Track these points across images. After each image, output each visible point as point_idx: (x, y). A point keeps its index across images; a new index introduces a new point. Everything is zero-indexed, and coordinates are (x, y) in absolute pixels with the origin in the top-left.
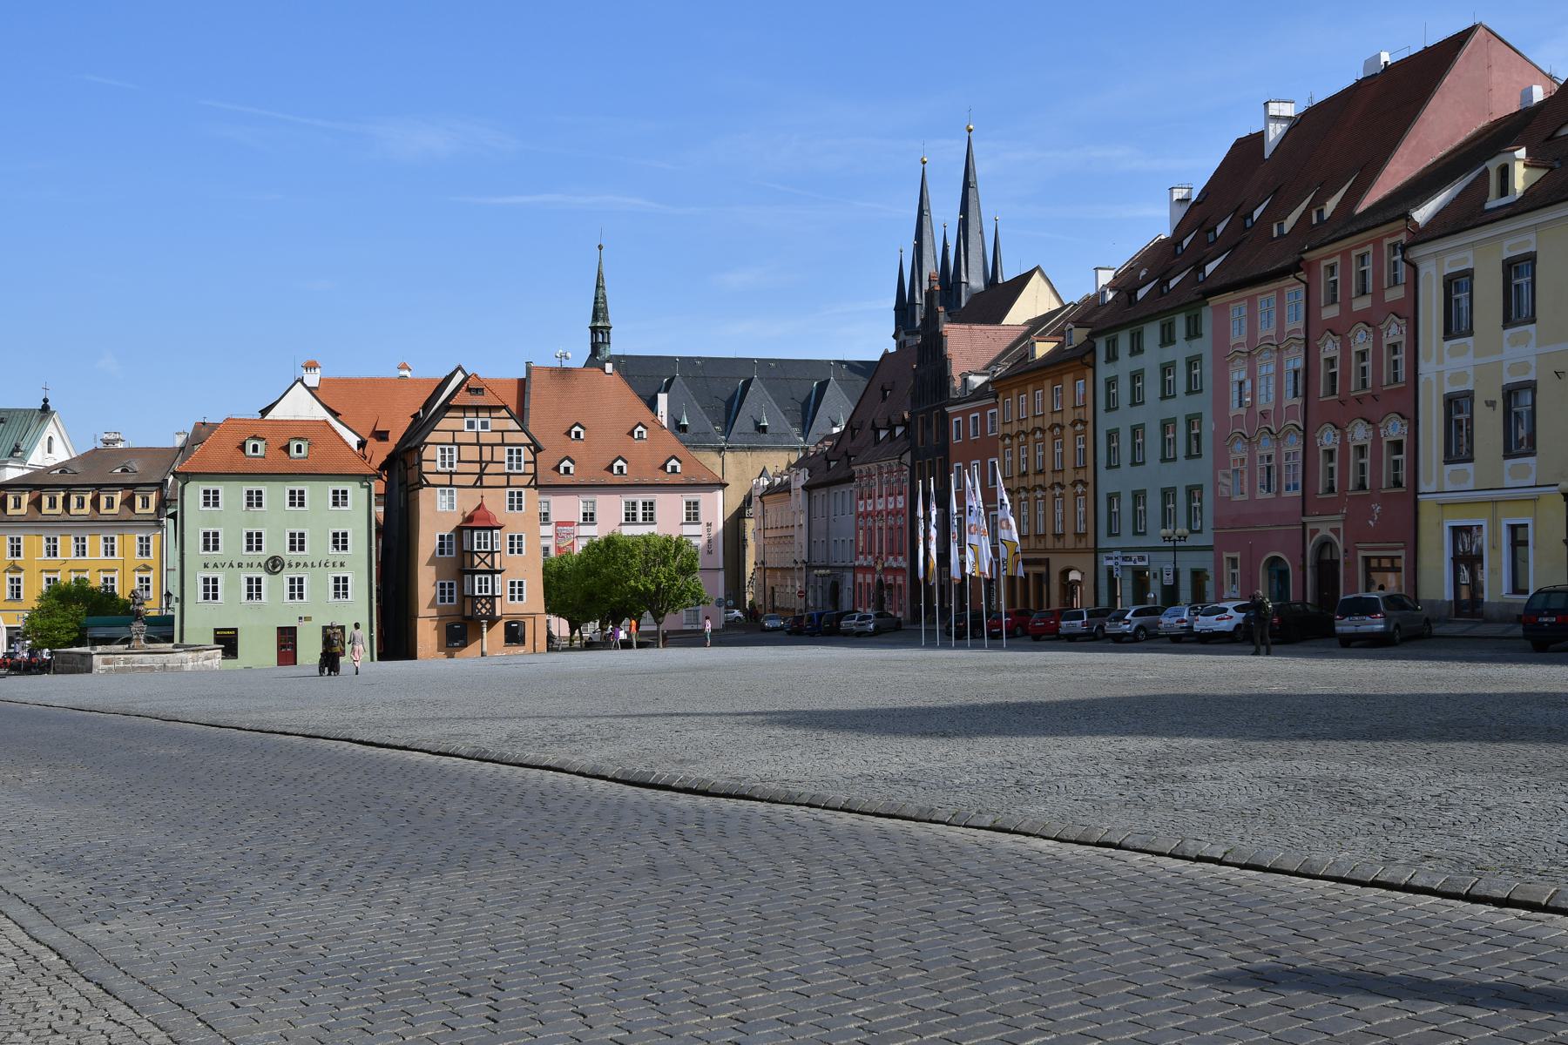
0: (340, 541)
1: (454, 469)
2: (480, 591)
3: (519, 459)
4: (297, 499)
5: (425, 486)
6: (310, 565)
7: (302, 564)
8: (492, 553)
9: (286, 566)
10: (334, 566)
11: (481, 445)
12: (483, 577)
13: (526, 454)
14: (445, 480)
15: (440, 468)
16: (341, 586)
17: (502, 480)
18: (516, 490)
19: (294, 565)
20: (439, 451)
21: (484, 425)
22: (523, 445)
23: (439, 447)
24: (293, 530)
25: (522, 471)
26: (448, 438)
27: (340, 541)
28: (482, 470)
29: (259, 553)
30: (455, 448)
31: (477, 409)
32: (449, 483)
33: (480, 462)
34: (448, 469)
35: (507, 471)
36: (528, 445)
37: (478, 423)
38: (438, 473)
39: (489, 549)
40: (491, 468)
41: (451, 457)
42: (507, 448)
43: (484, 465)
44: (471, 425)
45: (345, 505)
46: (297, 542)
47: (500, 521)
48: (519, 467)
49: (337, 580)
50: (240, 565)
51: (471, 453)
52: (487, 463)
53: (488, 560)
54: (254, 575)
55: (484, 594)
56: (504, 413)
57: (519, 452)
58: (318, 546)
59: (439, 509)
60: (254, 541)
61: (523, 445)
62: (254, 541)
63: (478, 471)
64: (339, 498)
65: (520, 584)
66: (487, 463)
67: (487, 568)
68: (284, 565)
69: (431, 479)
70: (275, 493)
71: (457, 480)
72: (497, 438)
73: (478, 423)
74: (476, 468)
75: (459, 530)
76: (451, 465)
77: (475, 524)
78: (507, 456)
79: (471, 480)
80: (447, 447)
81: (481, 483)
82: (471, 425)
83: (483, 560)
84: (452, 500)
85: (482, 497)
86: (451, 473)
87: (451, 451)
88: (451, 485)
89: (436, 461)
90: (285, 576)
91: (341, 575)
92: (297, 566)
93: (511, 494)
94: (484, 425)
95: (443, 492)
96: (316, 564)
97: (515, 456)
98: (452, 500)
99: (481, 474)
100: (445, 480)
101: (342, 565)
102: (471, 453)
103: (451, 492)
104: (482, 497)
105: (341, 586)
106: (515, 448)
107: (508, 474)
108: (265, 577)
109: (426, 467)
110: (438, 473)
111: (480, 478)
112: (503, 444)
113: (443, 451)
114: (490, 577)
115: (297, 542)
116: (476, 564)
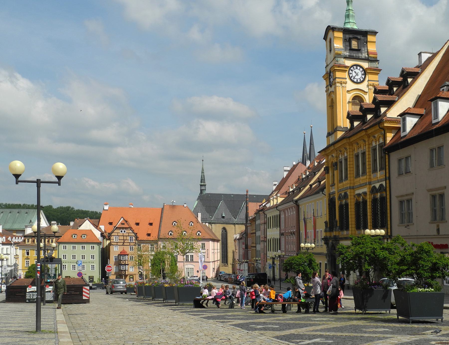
0: (93, 257)
1: (118, 241)
2: (123, 269)
3: (132, 239)
4: (83, 248)
11: (124, 236)
13: (134, 238)
14: (116, 244)
15: (115, 241)
16: (93, 267)
17: (129, 244)
18: (131, 246)
20: (114, 238)
21: (125, 232)
22: (133, 236)
23: (114, 236)
24: (82, 255)
25: (133, 242)
26: (116, 234)
27: (93, 257)
28: (124, 241)
29: (75, 259)
30: (118, 237)
31: (123, 228)
33: (124, 240)
34: (116, 241)
35: (129, 242)
36: (134, 236)
37: (123, 231)
40: (126, 241)
41: (117, 239)
42: (129, 237)
44: (122, 231)
45: (94, 249)
46: (83, 257)
47: (128, 253)
48: (132, 241)
49: (92, 266)
50: (71, 262)
51: (122, 238)
52: (125, 240)
56: (129, 229)
57: (132, 238)
58: (88, 258)
59: (115, 250)
60: (74, 257)
61: (133, 236)
62: (74, 257)
64: (93, 248)
66: (125, 240)
70: (79, 247)
71: (118, 244)
72: (127, 234)
73: (123, 231)
74: (123, 241)
75: (119, 255)
76: (117, 240)
77: (123, 254)
78: (129, 238)
79: (122, 244)
80: (116, 236)
82: (122, 231)
84: (117, 248)
86: (117, 242)
87: (117, 237)
88: (117, 245)
91: (93, 265)
94: (125, 232)
95: (115, 247)
97: (131, 238)
98: (117, 248)
99: (124, 243)
100: (116, 244)
101: (93, 262)
102: (122, 238)
103: (117, 247)
105: (93, 267)
106: (131, 237)
109: (112, 241)
111: (124, 244)
112: (129, 236)
113: (115, 237)
115: (83, 257)
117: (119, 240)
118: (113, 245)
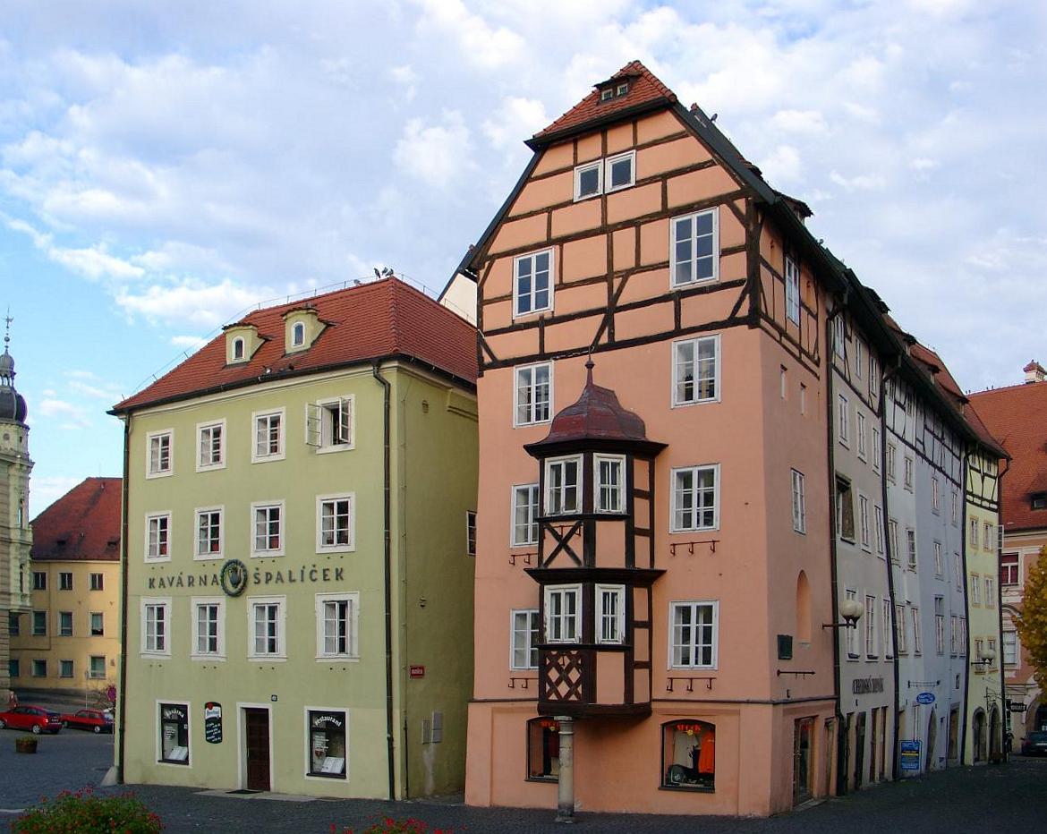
5: (490, 366)
6: (285, 577)
7: (275, 575)
8: (588, 521)
9: (251, 580)
10: (325, 580)
12: (563, 589)
17: (661, 317)
18: (695, 341)
19: (263, 578)
28: (613, 298)
32: (537, 352)
33: (607, 278)
34: (534, 313)
38: (515, 328)
39: (579, 510)
40: (636, 289)
41: (542, 281)
43: (617, 282)
51: (587, 258)
53: (577, 544)
54: (209, 601)
55: (565, 639)
63: (604, 303)
65: (707, 613)
67: (572, 565)
68: (246, 579)
69: (502, 347)
71: (557, 338)
74: (597, 296)
76: (542, 301)
80: (533, 256)
81: (611, 335)
83: (563, 543)
85: (590, 366)
86: (542, 323)
87: (543, 263)
88: (543, 356)
89: (509, 297)
90: (251, 600)
92: (267, 582)
93: (687, 352)
96: (297, 576)
99: (609, 313)
104: (590, 366)
107: (677, 297)
108: (222, 602)
110: (515, 328)
111: (608, 323)
114: (578, 589)
116: (546, 555)
117: (561, 286)
118: (509, 363)
